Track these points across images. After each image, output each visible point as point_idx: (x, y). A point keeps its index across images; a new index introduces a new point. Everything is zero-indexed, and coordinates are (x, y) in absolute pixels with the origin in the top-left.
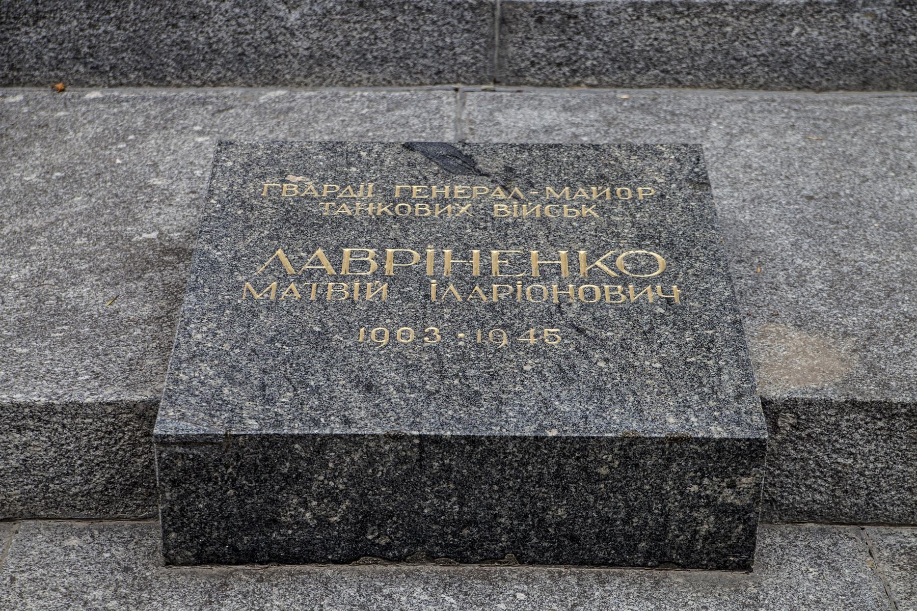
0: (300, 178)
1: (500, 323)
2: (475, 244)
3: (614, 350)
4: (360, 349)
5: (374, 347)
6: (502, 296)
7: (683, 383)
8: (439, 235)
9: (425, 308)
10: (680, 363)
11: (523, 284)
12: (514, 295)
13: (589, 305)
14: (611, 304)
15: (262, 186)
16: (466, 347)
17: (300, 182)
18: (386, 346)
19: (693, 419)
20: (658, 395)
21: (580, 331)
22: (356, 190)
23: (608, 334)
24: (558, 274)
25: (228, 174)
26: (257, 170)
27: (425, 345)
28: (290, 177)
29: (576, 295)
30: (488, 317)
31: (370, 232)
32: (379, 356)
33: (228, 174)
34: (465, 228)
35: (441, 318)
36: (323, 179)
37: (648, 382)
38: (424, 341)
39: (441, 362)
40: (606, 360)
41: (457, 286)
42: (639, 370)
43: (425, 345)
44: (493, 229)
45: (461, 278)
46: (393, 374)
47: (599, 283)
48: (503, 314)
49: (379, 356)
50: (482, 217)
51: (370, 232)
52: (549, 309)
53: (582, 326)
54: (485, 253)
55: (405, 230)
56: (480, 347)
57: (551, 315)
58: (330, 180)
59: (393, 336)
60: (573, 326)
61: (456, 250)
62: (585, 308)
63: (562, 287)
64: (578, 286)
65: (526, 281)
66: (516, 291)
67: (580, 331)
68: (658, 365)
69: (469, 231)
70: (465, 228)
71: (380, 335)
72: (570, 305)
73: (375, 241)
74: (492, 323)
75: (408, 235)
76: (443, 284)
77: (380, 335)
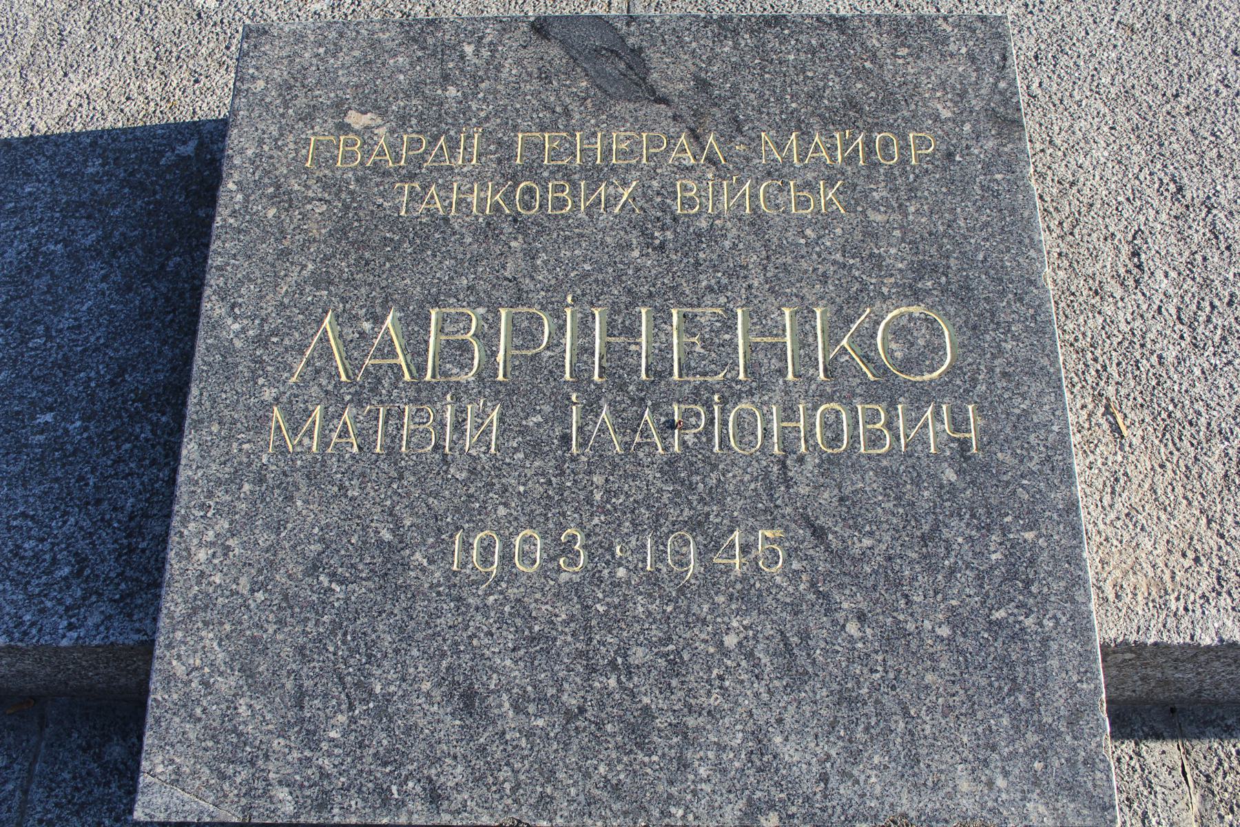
0: (366, 119)
1: (687, 513)
2: (644, 289)
3: (875, 587)
4: (454, 592)
5: (476, 583)
6: (690, 438)
7: (984, 682)
8: (587, 267)
9: (563, 473)
10: (982, 623)
11: (724, 400)
12: (708, 431)
13: (832, 461)
14: (869, 457)
15: (307, 141)
16: (628, 583)
17: (367, 128)
18: (498, 581)
19: (1001, 782)
20: (945, 716)
21: (819, 533)
22: (453, 145)
23: (867, 542)
24: (782, 372)
25: (256, 113)
26: (301, 102)
27: (564, 577)
28: (356, 119)
29: (810, 433)
30: (666, 496)
31: (475, 261)
32: (484, 609)
33: (256, 113)
34: (629, 246)
35: (589, 501)
36: (403, 120)
37: (929, 678)
38: (559, 570)
39: (587, 628)
40: (861, 617)
41: (615, 413)
42: (913, 646)
43: (564, 577)
44: (673, 254)
45: (622, 387)
46: (508, 662)
47: (848, 401)
48: (692, 488)
49: (484, 609)
50: (656, 223)
51: (475, 261)
52: (767, 473)
53: (821, 521)
54: (659, 317)
55: (531, 255)
56: (653, 580)
57: (770, 489)
58: (414, 121)
59: (507, 558)
60: (810, 524)
61: (614, 309)
62: (829, 464)
63: (789, 412)
64: (815, 408)
65: (731, 395)
66: (711, 422)
67: (819, 533)
68: (945, 631)
69: (636, 253)
70: (629, 246)
71: (487, 549)
72: (801, 460)
73: (482, 286)
74: (673, 512)
75: (535, 268)
76: (591, 408)
77: (487, 549)
